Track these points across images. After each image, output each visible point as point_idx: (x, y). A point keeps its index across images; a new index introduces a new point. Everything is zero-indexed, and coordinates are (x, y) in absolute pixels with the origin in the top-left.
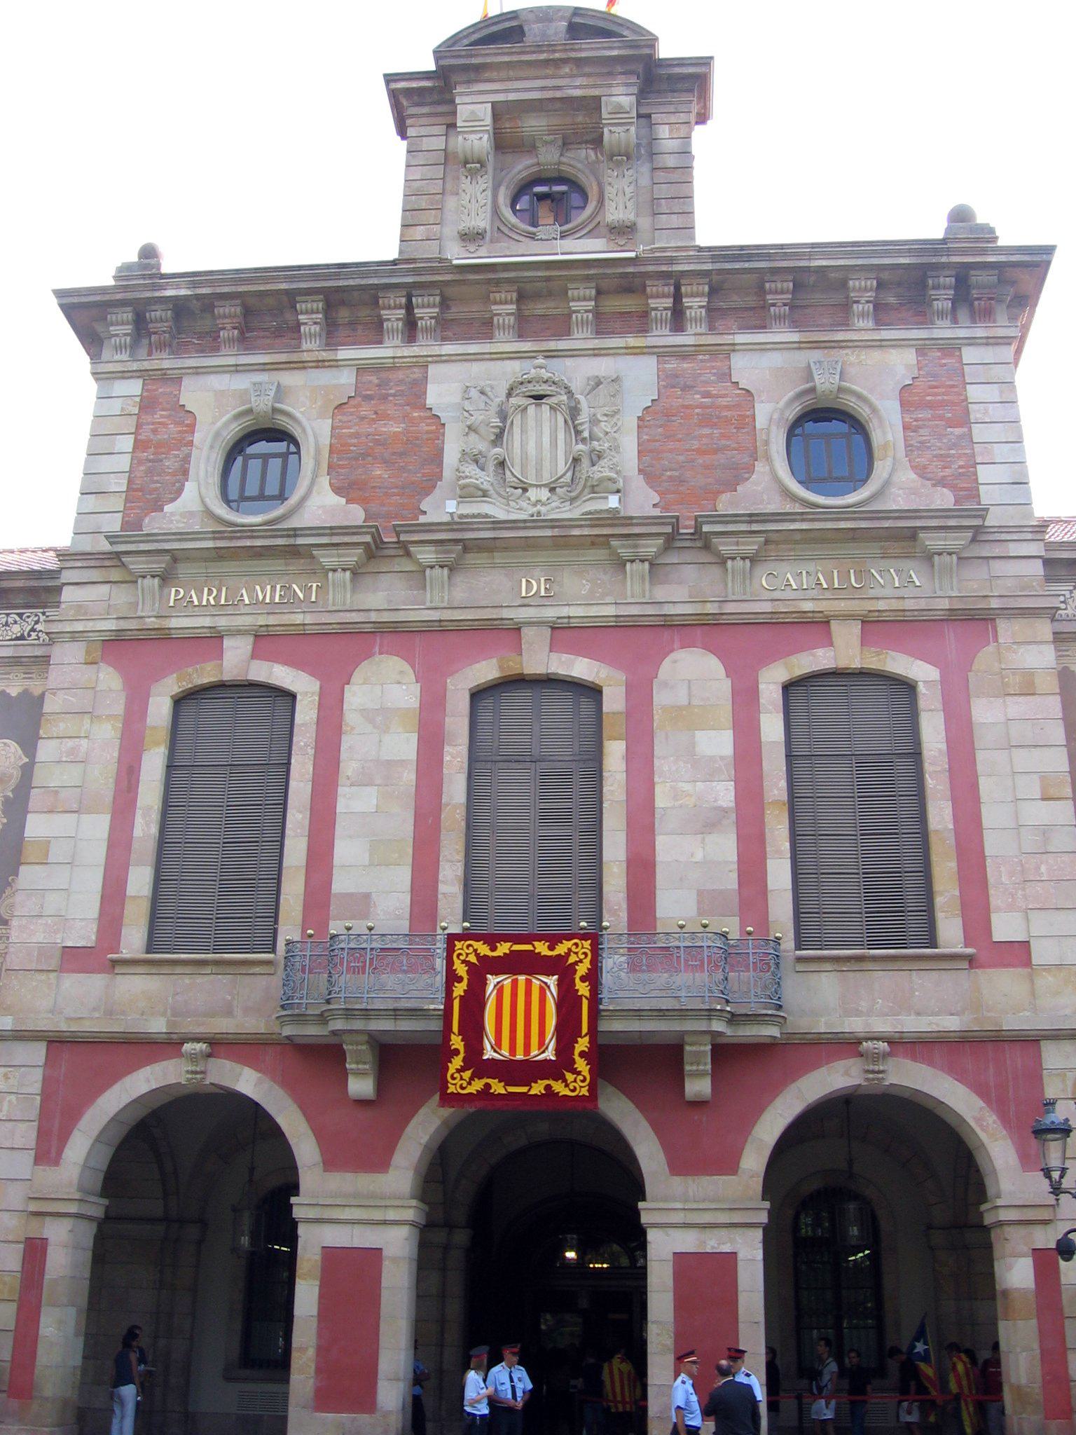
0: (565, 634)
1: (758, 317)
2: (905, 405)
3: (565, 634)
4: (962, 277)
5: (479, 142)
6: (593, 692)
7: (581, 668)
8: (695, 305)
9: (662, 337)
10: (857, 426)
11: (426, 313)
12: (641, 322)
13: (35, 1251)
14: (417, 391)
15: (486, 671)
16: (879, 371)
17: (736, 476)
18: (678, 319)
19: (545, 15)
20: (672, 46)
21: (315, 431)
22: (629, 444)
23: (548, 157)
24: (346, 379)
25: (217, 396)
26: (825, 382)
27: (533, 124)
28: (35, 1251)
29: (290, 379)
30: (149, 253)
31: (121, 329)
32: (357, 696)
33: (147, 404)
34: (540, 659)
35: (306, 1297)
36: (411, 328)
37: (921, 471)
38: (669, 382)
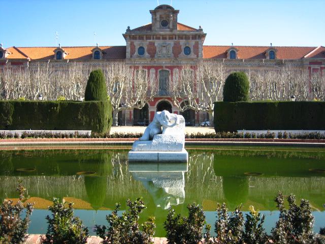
0: (166, 67)
1: (182, 39)
2: (194, 47)
3: (166, 67)
4: (199, 36)
5: (158, 19)
6: (168, 71)
7: (168, 69)
8: (177, 37)
9: (174, 40)
10: (190, 49)
11: (155, 37)
12: (172, 39)
13: (130, 112)
14: (154, 44)
15: (160, 70)
16: (192, 43)
17: (180, 53)
18: (176, 39)
19: (164, 6)
20: (176, 9)
21: (146, 48)
22: (171, 50)
23: (164, 19)
24: (148, 43)
25: (137, 43)
26: (187, 46)
27: (163, 16)
28: (130, 112)
29: (143, 42)
30: (129, 27)
31: (128, 37)
32: (151, 71)
33: (131, 44)
34: (165, 69)
35: (150, 114)
36: (153, 39)
37: (194, 53)
38: (175, 44)
